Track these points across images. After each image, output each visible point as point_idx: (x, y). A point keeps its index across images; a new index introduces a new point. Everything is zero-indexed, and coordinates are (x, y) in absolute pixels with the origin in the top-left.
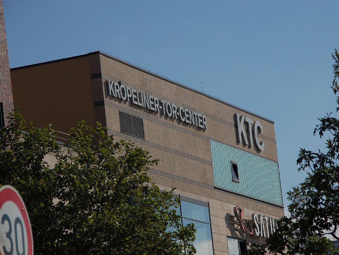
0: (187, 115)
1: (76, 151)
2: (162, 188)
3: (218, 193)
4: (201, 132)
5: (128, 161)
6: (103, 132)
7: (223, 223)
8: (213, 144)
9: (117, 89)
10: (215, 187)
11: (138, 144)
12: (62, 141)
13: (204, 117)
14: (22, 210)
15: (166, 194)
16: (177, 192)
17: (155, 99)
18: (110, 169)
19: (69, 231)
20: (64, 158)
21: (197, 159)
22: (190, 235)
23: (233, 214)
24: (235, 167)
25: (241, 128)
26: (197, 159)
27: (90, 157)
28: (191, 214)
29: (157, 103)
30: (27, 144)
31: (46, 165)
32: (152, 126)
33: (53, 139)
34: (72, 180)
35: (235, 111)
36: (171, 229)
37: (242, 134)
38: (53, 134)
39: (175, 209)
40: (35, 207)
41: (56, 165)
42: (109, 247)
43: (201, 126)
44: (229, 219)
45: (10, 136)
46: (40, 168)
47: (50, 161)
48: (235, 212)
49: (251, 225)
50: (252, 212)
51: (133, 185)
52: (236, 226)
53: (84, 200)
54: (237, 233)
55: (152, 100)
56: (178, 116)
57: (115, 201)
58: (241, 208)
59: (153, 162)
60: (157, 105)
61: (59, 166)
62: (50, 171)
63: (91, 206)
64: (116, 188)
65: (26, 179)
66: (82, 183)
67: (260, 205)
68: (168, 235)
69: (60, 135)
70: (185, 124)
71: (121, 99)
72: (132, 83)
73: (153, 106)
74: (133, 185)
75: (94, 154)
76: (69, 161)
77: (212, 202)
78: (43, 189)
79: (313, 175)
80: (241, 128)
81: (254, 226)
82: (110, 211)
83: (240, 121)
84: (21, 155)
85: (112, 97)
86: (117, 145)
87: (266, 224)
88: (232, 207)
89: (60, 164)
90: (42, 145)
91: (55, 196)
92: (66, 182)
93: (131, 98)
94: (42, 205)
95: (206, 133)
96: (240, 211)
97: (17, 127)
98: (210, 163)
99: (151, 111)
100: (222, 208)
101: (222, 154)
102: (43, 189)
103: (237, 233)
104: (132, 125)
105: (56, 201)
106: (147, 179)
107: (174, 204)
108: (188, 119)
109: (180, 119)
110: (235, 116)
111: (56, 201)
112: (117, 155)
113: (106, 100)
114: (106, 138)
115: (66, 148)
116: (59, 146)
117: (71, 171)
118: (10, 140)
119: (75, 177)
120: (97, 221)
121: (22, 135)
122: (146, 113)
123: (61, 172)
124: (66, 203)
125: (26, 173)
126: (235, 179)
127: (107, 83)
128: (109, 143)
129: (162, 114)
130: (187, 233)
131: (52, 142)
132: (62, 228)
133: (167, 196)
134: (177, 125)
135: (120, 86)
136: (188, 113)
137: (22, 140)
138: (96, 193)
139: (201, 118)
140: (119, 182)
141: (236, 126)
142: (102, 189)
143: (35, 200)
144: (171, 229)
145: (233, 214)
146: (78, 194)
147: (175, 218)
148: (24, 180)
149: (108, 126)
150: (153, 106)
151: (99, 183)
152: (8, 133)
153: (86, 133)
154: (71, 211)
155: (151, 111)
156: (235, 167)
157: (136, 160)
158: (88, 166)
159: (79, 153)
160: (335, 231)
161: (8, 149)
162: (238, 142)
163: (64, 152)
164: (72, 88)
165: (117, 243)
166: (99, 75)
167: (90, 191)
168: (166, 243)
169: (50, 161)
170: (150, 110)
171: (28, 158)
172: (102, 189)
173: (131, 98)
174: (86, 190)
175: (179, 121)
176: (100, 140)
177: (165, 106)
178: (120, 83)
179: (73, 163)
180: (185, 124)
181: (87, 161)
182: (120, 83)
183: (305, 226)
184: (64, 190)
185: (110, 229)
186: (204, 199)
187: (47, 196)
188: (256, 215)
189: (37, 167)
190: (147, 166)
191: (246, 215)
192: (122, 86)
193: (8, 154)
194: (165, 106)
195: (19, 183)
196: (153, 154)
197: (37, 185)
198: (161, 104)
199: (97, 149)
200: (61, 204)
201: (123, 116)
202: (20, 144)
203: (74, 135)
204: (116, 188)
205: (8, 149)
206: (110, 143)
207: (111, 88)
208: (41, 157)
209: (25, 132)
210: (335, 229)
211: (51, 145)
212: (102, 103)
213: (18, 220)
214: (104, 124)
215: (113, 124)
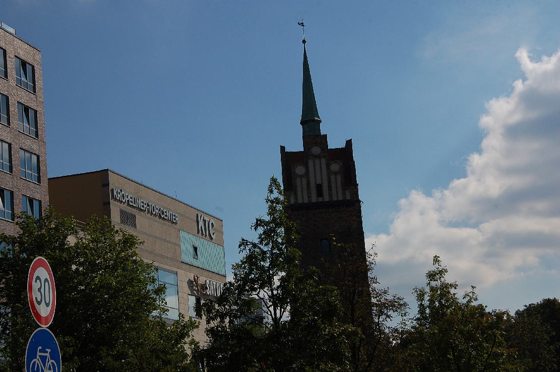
0: (165, 214)
1: (89, 234)
2: (146, 261)
3: (184, 265)
4: (174, 225)
5: (124, 242)
6: (108, 222)
7: (186, 285)
8: (182, 234)
9: (119, 194)
10: (182, 262)
11: (130, 231)
12: (81, 227)
13: (176, 215)
14: (49, 274)
15: (147, 264)
16: (156, 264)
17: (145, 202)
18: (112, 248)
19: (83, 288)
20: (80, 239)
21: (170, 242)
22: (162, 291)
23: (193, 280)
24: (195, 249)
25: (201, 223)
26: (170, 242)
27: (98, 239)
28: (164, 278)
29: (145, 205)
30: (56, 229)
31: (68, 243)
32: (142, 220)
33: (74, 226)
34: (86, 253)
35: (197, 212)
36: (150, 287)
37: (201, 227)
38: (74, 223)
39: (154, 275)
40: (60, 271)
41: (75, 243)
42: (108, 299)
43: (175, 221)
44: (190, 283)
45: (45, 223)
46: (64, 244)
47: (71, 240)
48: (194, 279)
49: (204, 287)
50: (205, 279)
51: (126, 259)
52: (194, 287)
53: (93, 267)
54: (195, 292)
55: (143, 202)
56: (160, 214)
57: (114, 268)
58: (199, 276)
59: (141, 243)
60: (145, 206)
61: (77, 244)
62: (71, 247)
63: (97, 271)
64: (115, 260)
65: (55, 252)
66: (92, 256)
67: (211, 274)
68: (149, 291)
69: (79, 223)
70: (164, 219)
71: (122, 201)
72: (129, 192)
73: (143, 206)
74: (126, 259)
75: (102, 237)
76: (84, 241)
77: (179, 271)
78: (66, 259)
79: (408, 328)
80: (201, 223)
81: (206, 288)
82: (110, 275)
83: (201, 218)
84: (52, 236)
85: (116, 199)
86: (117, 231)
87: (215, 288)
88: (193, 275)
89: (78, 242)
90: (66, 229)
91: (73, 264)
92: (81, 255)
93: (128, 201)
94: (64, 269)
95: (177, 226)
96: (198, 278)
97: (50, 216)
98: (179, 246)
99: (141, 210)
100: (186, 276)
101: (187, 240)
102: (66, 259)
103: (195, 292)
104: (129, 219)
105: (74, 267)
106: (136, 255)
107: (154, 271)
108: (166, 216)
109: (160, 216)
110: (197, 215)
111: (74, 267)
112: (118, 238)
113: (112, 201)
114: (110, 227)
115: (82, 232)
116: (78, 231)
117: (85, 248)
118: (45, 225)
119: (88, 252)
120: (101, 281)
121: (53, 222)
122: (138, 211)
123: (78, 248)
124: (81, 269)
125: (55, 248)
126: (196, 257)
127: (112, 190)
128: (112, 230)
129: (149, 212)
130: (160, 290)
131: (73, 228)
132: (77, 285)
133: (149, 266)
134: (150, 216)
135: (121, 192)
136: (166, 212)
137: (53, 226)
138: (101, 262)
139: (175, 216)
140: (117, 256)
141: (198, 222)
142: (106, 260)
143: (60, 266)
144: (150, 287)
145: (193, 280)
146: (89, 263)
147: (153, 280)
148: (53, 252)
149: (112, 219)
150: (143, 206)
151: (104, 256)
152: (44, 221)
153: (97, 222)
154: (84, 274)
155: (141, 210)
156: (195, 249)
157: (129, 242)
158: (97, 245)
159: (91, 236)
160: (259, 293)
161: (43, 231)
162: (198, 232)
163: (81, 234)
164: (88, 194)
165: (114, 296)
166: (108, 185)
167: (97, 262)
168: (146, 296)
169: (71, 240)
170: (141, 209)
171: (57, 238)
172: (106, 260)
173: (128, 201)
174: (95, 260)
175: (160, 217)
176: (106, 228)
177: (209, 224)
178: (121, 191)
179: (87, 243)
180: (164, 219)
181: (96, 241)
182: (121, 191)
183: (241, 289)
184: (79, 260)
185: (108, 287)
186: (175, 270)
187: (68, 263)
188: (208, 281)
189: (63, 244)
190: (136, 246)
191: (201, 281)
192: (123, 192)
193: (43, 235)
194: (209, 224)
195: (49, 254)
196: (141, 238)
197: (61, 256)
198: (148, 205)
199: (104, 233)
200: (77, 269)
201: (122, 212)
202: (51, 229)
203: (89, 224)
204: (115, 260)
205: (43, 231)
206: (113, 230)
207: (115, 193)
208: (65, 237)
209: (55, 221)
210: (260, 291)
211: (72, 230)
212: (109, 203)
213: (46, 280)
214: (109, 217)
215: (115, 217)
